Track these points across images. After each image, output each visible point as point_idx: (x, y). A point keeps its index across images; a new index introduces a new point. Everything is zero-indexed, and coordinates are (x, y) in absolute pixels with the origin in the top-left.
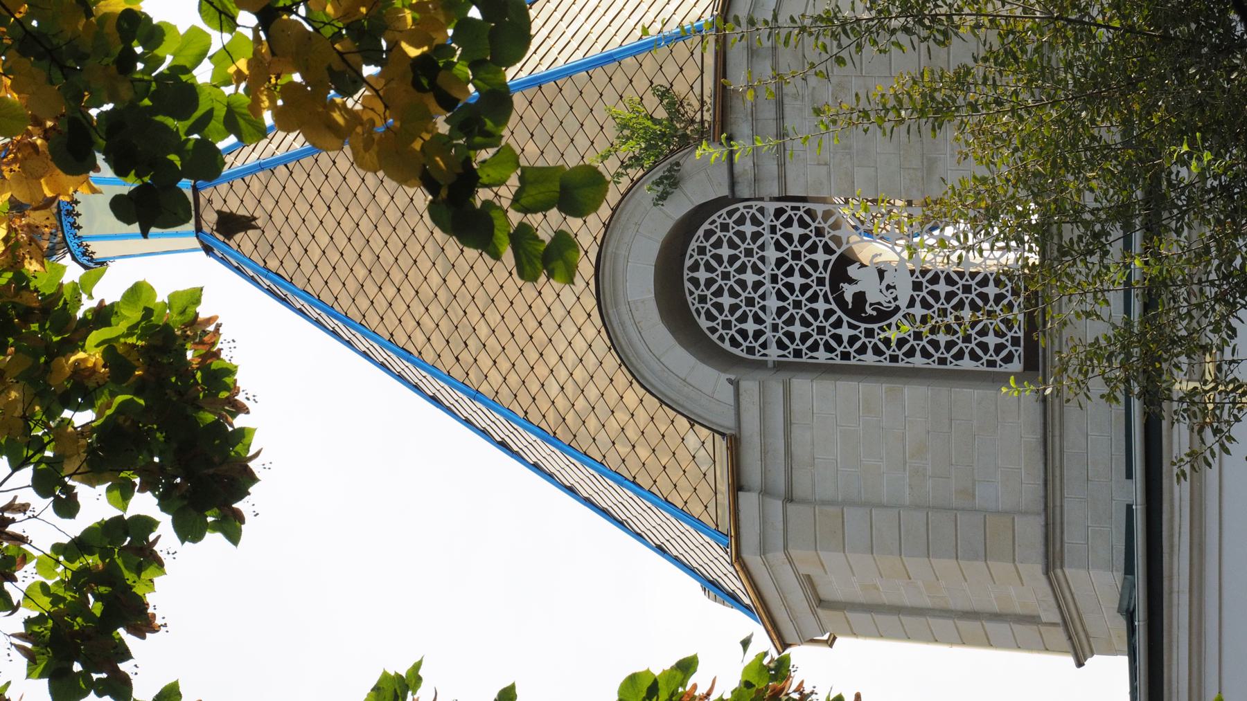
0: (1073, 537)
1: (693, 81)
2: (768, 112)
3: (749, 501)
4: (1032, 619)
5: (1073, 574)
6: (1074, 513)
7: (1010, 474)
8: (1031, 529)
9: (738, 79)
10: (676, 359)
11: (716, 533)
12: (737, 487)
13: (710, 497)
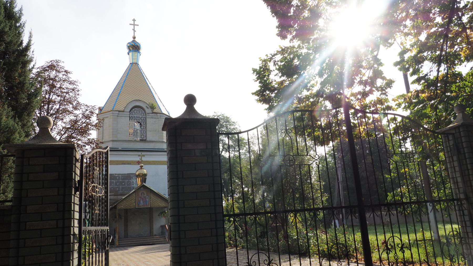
0: (115, 143)
1: (155, 111)
2: (155, 117)
3: (118, 112)
4: (103, 139)
5: (111, 143)
6: (118, 143)
7: (120, 137)
8: (116, 139)
9: (158, 114)
10: (131, 107)
11: (113, 108)
12: (119, 111)
13: (117, 108)
